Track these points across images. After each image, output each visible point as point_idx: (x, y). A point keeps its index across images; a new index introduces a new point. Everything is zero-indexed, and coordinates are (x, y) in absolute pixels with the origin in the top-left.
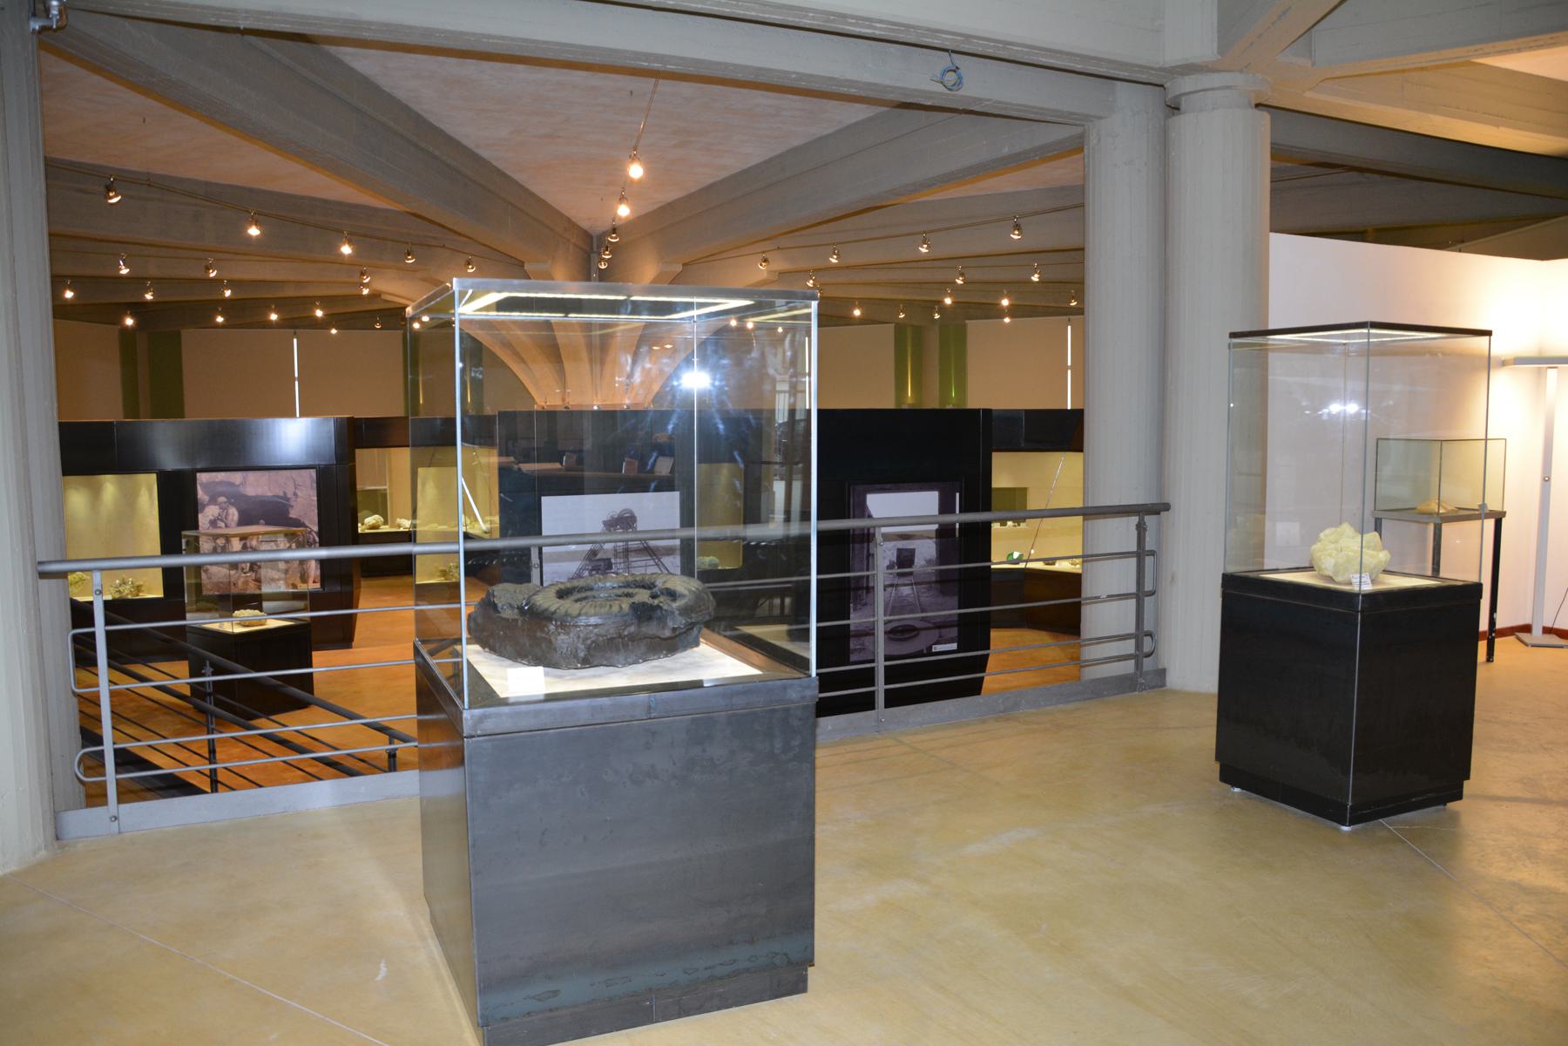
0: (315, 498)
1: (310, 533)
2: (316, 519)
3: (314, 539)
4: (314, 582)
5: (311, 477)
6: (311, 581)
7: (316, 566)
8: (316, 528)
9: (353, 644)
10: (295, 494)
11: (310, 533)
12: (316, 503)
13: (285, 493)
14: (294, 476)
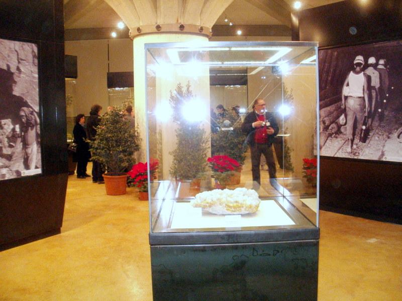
0: (37, 76)
1: (32, 113)
2: (37, 99)
3: (36, 121)
4: (37, 167)
5: (33, 51)
6: (33, 165)
7: (38, 150)
8: (37, 109)
9: (62, 229)
10: (18, 69)
11: (32, 113)
12: (37, 81)
13: (8, 66)
14: (17, 48)
